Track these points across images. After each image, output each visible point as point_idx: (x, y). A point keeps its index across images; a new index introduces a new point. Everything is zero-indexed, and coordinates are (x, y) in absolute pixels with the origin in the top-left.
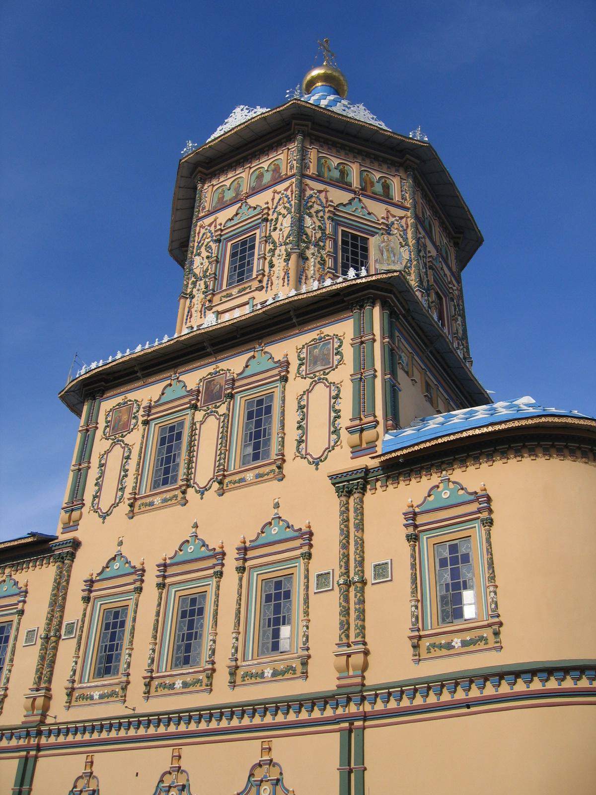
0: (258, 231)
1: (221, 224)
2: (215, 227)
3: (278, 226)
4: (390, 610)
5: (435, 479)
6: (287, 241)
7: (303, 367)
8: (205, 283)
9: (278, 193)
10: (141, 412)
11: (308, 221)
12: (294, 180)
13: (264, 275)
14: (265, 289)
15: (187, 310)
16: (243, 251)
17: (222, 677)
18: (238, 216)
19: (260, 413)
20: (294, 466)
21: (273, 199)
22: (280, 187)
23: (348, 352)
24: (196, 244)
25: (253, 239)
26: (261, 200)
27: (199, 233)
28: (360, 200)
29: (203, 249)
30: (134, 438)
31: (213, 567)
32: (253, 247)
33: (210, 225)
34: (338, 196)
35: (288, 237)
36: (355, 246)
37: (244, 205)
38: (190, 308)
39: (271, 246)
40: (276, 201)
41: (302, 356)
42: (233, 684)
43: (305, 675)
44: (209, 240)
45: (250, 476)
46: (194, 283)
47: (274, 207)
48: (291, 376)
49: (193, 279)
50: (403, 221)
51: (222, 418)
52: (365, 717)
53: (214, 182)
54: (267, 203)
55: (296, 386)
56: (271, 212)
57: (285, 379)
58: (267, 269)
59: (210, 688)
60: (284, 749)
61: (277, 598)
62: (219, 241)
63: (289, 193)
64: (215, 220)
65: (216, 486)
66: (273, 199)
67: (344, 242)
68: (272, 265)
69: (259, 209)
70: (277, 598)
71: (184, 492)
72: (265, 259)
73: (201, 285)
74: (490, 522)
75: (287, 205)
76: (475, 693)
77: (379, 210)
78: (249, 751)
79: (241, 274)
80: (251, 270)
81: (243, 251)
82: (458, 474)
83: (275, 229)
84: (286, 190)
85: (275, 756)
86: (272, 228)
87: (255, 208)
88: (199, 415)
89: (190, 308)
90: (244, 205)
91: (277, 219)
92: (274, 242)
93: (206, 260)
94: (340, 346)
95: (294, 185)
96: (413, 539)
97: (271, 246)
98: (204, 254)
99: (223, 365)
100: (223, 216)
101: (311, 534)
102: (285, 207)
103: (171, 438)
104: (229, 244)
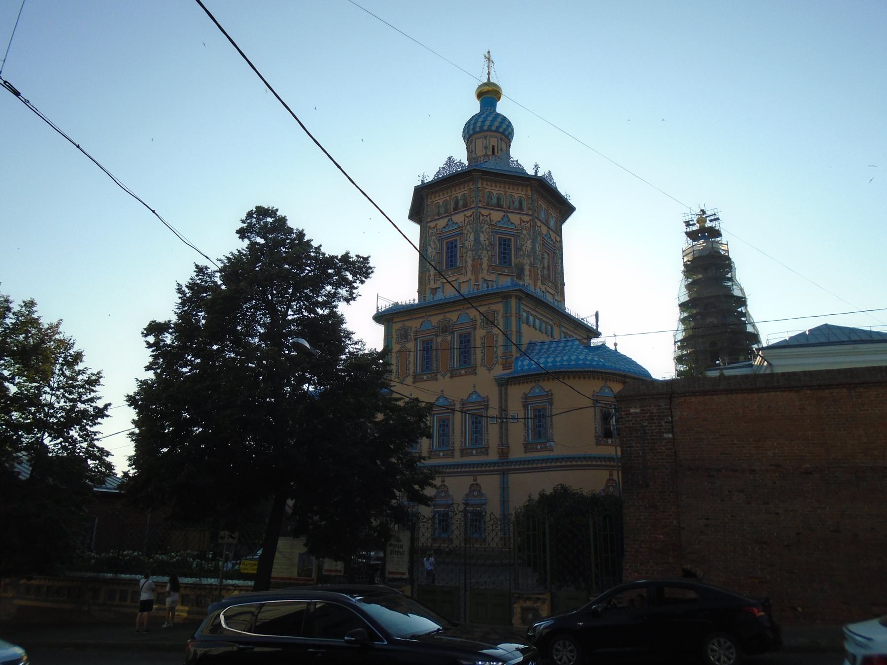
4: (517, 433)
5: (533, 384)
10: (412, 334)
11: (482, 237)
17: (457, 453)
19: (466, 341)
20: (481, 370)
22: (469, 213)
26: (458, 218)
30: (410, 345)
32: (456, 246)
34: (496, 216)
36: (505, 245)
39: (465, 250)
42: (462, 456)
43: (487, 454)
45: (463, 372)
48: (478, 327)
50: (528, 225)
52: (509, 470)
55: (480, 333)
57: (475, 329)
59: (453, 457)
60: (481, 480)
61: (477, 423)
65: (449, 375)
67: (500, 244)
68: (466, 262)
70: (477, 423)
74: (551, 404)
76: (544, 465)
77: (515, 218)
78: (469, 480)
82: (541, 383)
85: (479, 482)
88: (439, 339)
89: (429, 276)
96: (525, 406)
98: (433, 246)
99: (448, 315)
100: (442, 223)
101: (488, 400)
103: (427, 348)
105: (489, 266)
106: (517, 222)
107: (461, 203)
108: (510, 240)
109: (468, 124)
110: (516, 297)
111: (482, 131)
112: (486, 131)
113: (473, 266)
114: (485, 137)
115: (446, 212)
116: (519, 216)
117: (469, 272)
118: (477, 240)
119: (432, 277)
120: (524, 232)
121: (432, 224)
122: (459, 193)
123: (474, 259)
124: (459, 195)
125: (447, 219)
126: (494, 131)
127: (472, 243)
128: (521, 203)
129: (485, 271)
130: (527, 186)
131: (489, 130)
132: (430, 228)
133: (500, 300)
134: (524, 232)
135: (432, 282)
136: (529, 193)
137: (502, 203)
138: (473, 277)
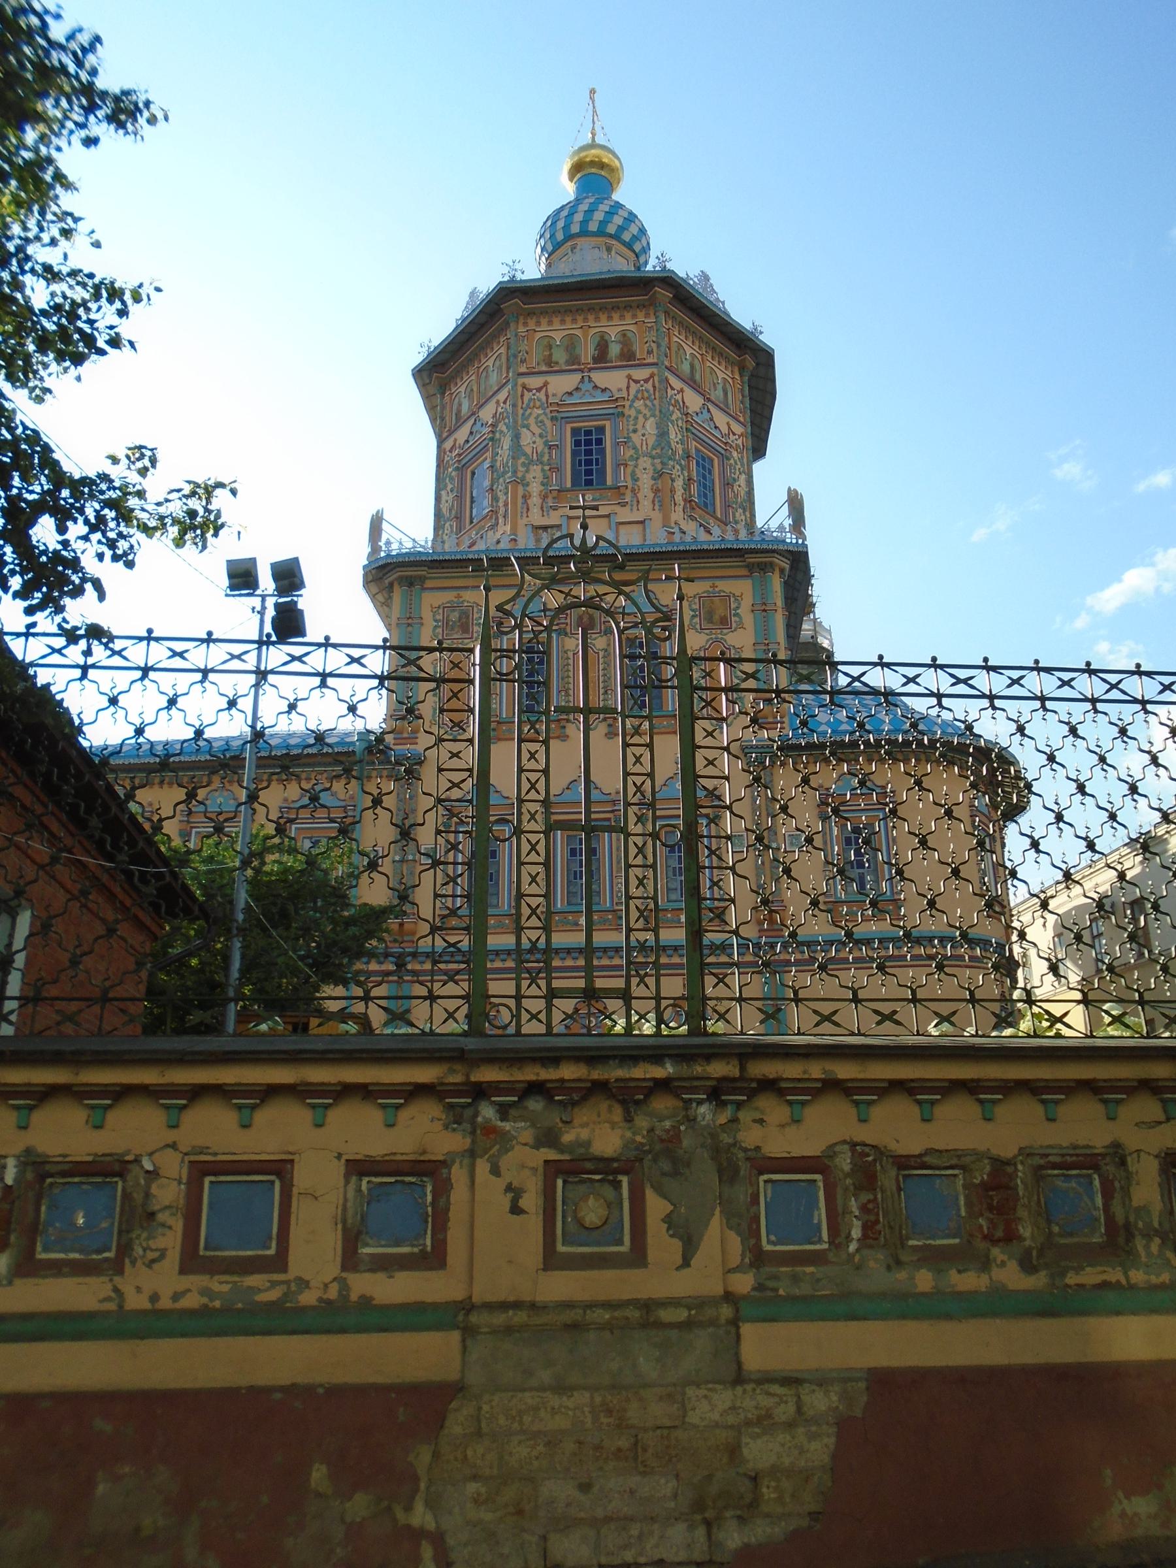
0: (608, 424)
1: (554, 395)
2: (547, 396)
3: (639, 426)
6: (654, 452)
7: (697, 620)
8: (543, 470)
9: (637, 382)
11: (674, 435)
12: (655, 370)
13: (627, 487)
14: (628, 507)
15: (520, 500)
16: (588, 443)
18: (581, 394)
21: (628, 388)
22: (640, 374)
23: (748, 619)
24: (521, 412)
25: (601, 430)
26: (613, 380)
27: (522, 396)
28: (709, 411)
29: (532, 421)
31: (613, 811)
32: (599, 442)
33: (539, 390)
34: (694, 401)
35: (654, 448)
36: (704, 468)
37: (586, 379)
38: (524, 497)
40: (633, 391)
41: (694, 607)
44: (540, 412)
46: (527, 466)
47: (631, 397)
49: (522, 459)
51: (601, 654)
53: (532, 324)
54: (620, 390)
56: (627, 404)
58: (629, 479)
62: (552, 419)
63: (649, 386)
64: (546, 384)
66: (628, 388)
69: (608, 394)
71: (564, 727)
72: (626, 465)
73: (536, 472)
75: (648, 402)
77: (721, 419)
79: (589, 472)
80: (602, 472)
81: (588, 443)
83: (635, 431)
84: (646, 381)
86: (631, 428)
87: (604, 390)
90: (586, 379)
91: (636, 418)
92: (635, 448)
93: (538, 440)
94: (738, 608)
95: (656, 378)
97: (632, 452)
100: (561, 384)
102: (646, 405)
104: (569, 427)
105: (685, 500)
106: (725, 430)
107: (614, 350)
108: (712, 461)
109: (555, 217)
110: (782, 571)
111: (601, 233)
112: (611, 236)
113: (656, 491)
114: (609, 249)
115: (574, 360)
116: (726, 419)
117: (646, 504)
118: (663, 434)
119: (535, 500)
120: (735, 454)
121: (535, 382)
122: (613, 328)
123: (659, 475)
124: (613, 333)
125: (578, 376)
126: (624, 243)
127: (650, 444)
128: (726, 394)
129: (680, 509)
130: (733, 364)
131: (616, 237)
132: (524, 387)
133: (745, 572)
134: (735, 454)
135: (535, 512)
136: (737, 377)
137: (698, 377)
138: (657, 516)
